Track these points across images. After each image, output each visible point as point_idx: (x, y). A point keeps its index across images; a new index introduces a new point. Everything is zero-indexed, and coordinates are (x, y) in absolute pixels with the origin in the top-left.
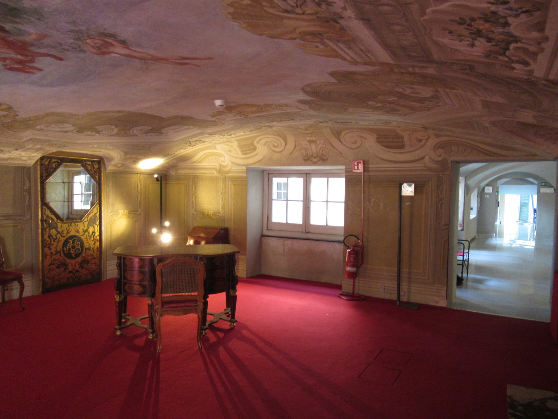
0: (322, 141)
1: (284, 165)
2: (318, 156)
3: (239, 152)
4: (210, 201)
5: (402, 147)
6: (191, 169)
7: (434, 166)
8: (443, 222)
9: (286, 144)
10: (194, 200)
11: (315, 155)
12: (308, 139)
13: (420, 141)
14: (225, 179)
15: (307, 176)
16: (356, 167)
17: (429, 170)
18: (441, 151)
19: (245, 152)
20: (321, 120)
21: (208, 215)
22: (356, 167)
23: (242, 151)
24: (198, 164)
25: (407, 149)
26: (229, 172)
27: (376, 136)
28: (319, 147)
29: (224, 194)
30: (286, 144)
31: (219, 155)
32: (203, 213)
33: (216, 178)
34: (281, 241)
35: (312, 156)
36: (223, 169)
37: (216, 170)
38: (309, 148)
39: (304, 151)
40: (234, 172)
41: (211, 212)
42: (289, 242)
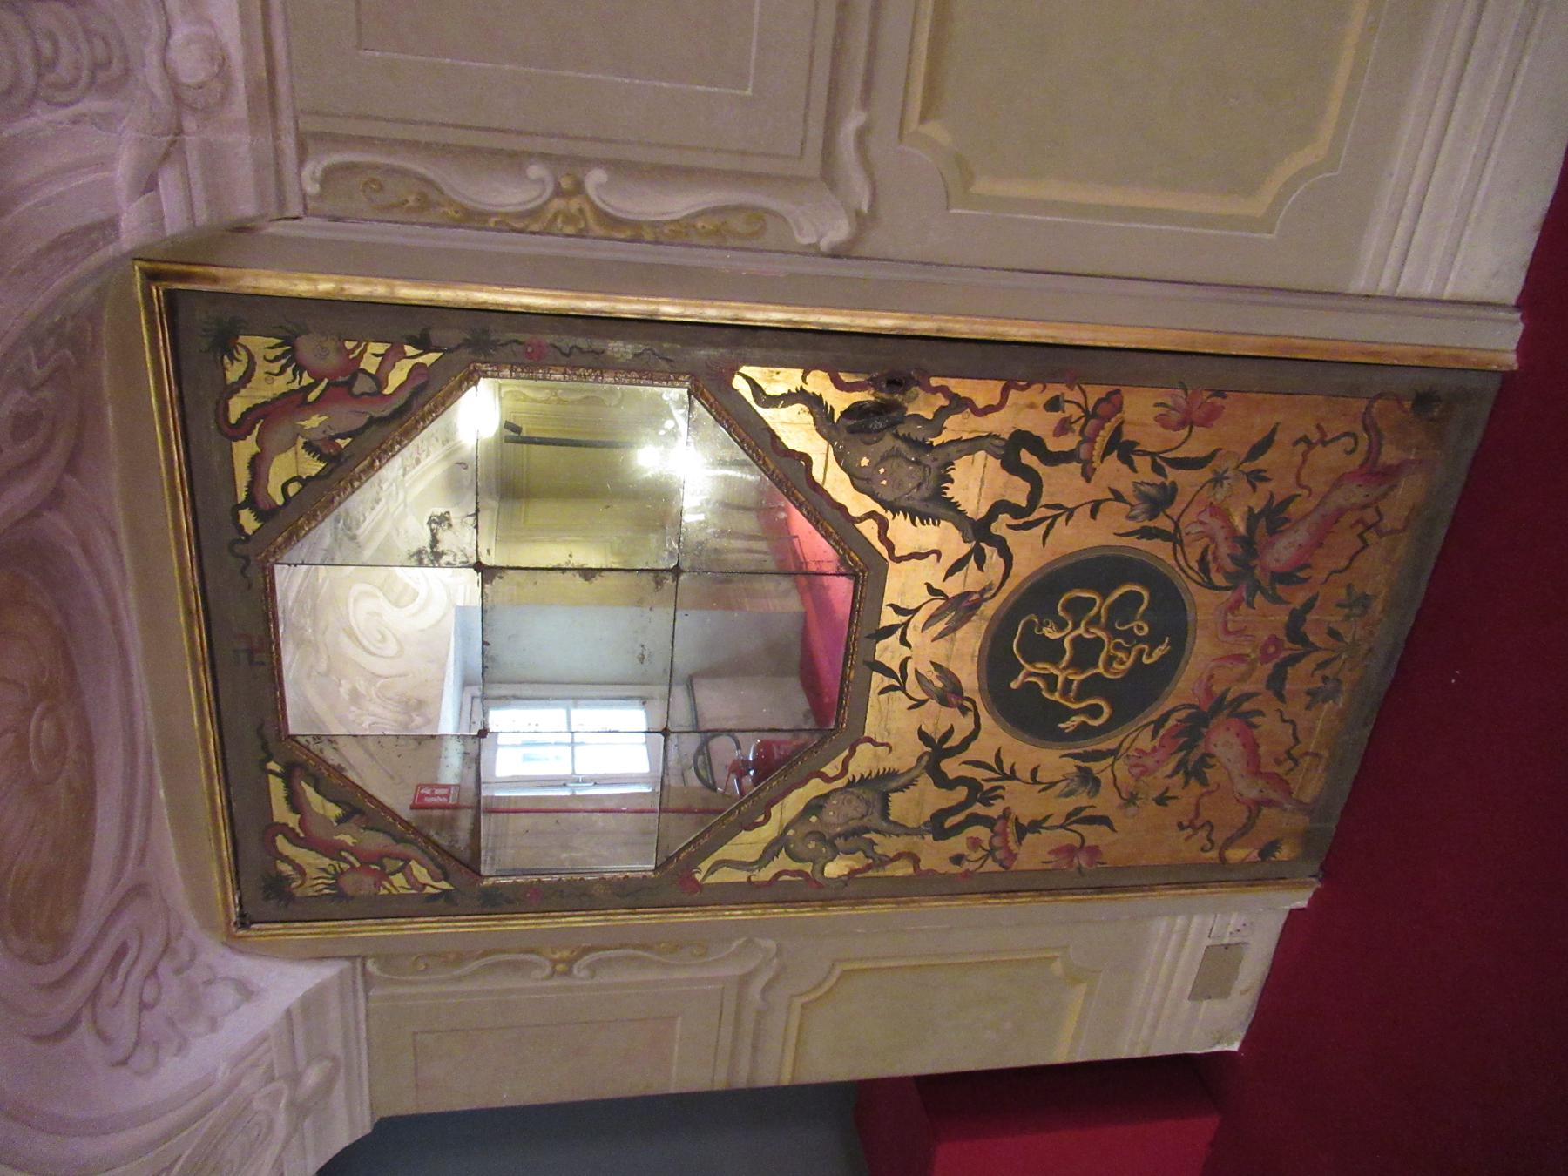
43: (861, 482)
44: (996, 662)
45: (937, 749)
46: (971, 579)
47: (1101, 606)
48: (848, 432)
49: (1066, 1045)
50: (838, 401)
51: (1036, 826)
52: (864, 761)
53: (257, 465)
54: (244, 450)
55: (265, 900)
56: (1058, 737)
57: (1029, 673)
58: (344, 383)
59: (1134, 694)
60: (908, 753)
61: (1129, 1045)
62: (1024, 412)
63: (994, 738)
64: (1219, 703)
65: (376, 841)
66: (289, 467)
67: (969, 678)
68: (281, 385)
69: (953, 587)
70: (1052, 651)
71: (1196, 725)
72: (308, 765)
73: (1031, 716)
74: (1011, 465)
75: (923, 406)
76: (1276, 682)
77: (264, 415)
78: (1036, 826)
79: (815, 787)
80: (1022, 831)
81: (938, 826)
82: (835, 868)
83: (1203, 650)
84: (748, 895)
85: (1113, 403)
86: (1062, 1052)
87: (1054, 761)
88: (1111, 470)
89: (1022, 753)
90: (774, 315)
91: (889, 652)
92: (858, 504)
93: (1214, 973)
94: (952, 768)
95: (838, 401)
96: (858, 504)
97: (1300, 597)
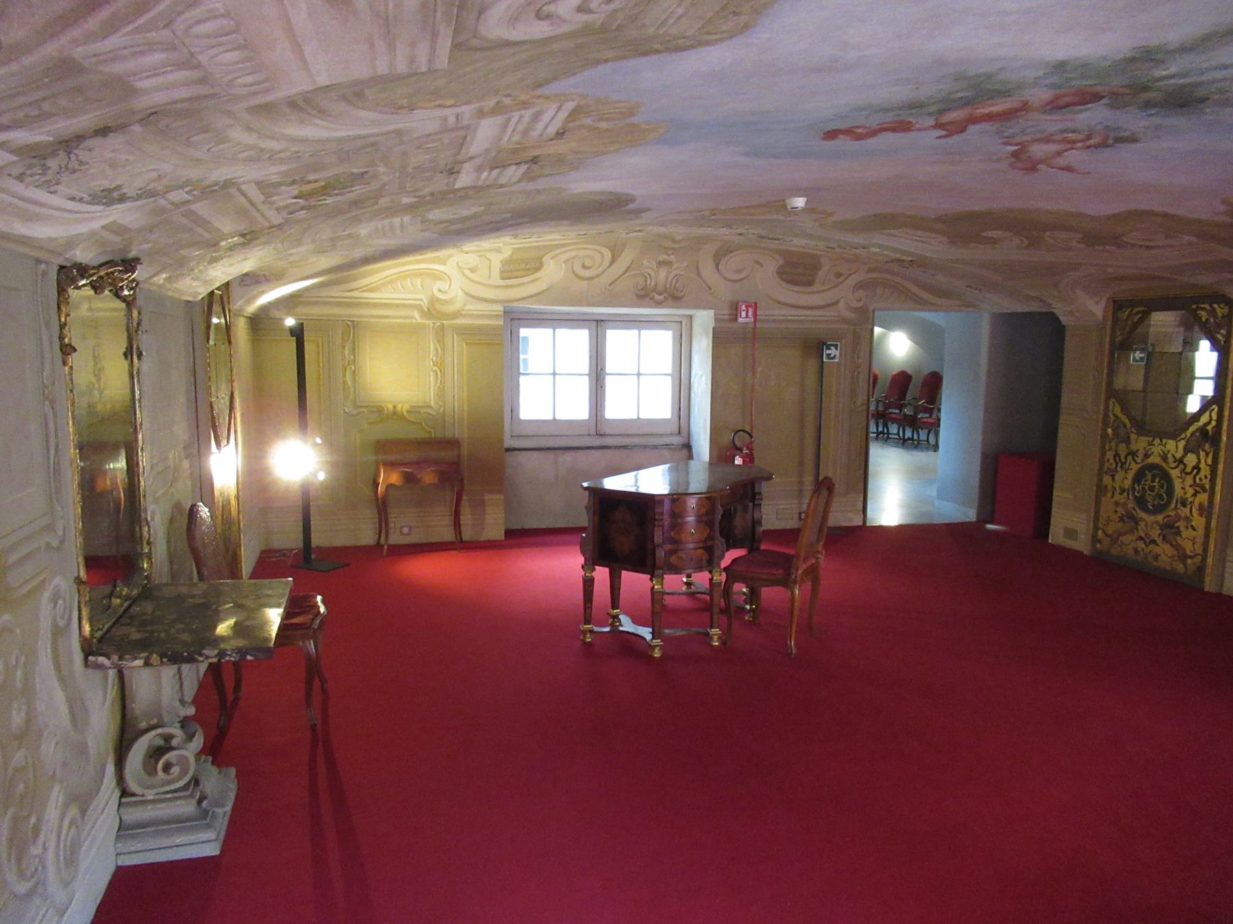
0: (686, 264)
1: (590, 305)
2: (665, 290)
3: (496, 272)
4: (400, 380)
5: (810, 283)
6: (339, 304)
7: (849, 315)
8: (859, 401)
9: (612, 263)
10: (349, 379)
11: (660, 288)
12: (662, 257)
13: (839, 275)
14: (441, 332)
15: (598, 326)
16: (744, 314)
17: (845, 321)
18: (861, 293)
19: (505, 275)
20: (763, 233)
21: (395, 413)
22: (744, 314)
23: (502, 272)
24: (365, 295)
25: (817, 286)
26: (457, 315)
27: (781, 262)
28: (674, 273)
29: (440, 364)
30: (612, 263)
31: (436, 276)
32: (380, 410)
33: (416, 330)
34: (551, 456)
35: (654, 290)
36: (437, 306)
37: (421, 311)
38: (652, 274)
39: (640, 280)
40: (471, 316)
41: (403, 408)
42: (568, 457)
43: (1193, 434)
44: (1153, 467)
45: (1133, 454)
46: (1171, 459)
47: (1162, 491)
48: (1203, 431)
49: (1058, 494)
50: (1209, 428)
51: (1113, 479)
52: (1133, 436)
53: (1203, 309)
54: (1207, 306)
55: (1118, 305)
56: (1133, 483)
57: (1149, 476)
58: (1219, 326)
59: (1141, 503)
60: (1134, 447)
61: (1055, 510)
62: (1205, 470)
63: (1135, 468)
64: (1137, 524)
65: (1128, 329)
66: (1203, 314)
67: (1150, 460)
68: (1220, 315)
69: (1169, 455)
70: (1153, 481)
71: (1132, 518)
72: (1145, 315)
73: (1139, 477)
74: (1194, 468)
75: (1207, 447)
76: (1141, 538)
77: (1213, 313)
78: (1113, 479)
79: (1129, 425)
80: (1113, 476)
81: (1117, 455)
82: (1110, 431)
83: (1151, 518)
84: (1107, 407)
85: (1205, 491)
86: (1055, 493)
87: (1127, 483)
88: (1191, 491)
89: (1131, 475)
90: (1226, 413)
91: (1157, 441)
92: (1188, 433)
93: (1070, 533)
94: (1130, 458)
95: (1209, 428)
96: (1188, 433)
97: (1159, 542)
